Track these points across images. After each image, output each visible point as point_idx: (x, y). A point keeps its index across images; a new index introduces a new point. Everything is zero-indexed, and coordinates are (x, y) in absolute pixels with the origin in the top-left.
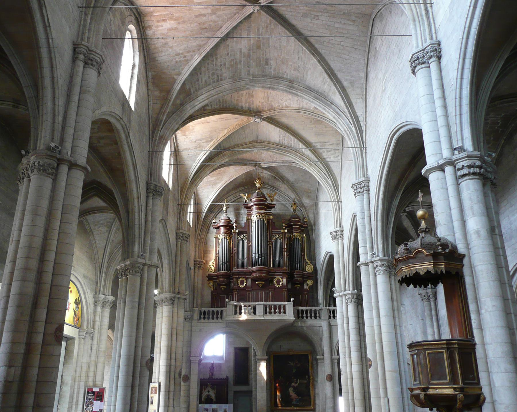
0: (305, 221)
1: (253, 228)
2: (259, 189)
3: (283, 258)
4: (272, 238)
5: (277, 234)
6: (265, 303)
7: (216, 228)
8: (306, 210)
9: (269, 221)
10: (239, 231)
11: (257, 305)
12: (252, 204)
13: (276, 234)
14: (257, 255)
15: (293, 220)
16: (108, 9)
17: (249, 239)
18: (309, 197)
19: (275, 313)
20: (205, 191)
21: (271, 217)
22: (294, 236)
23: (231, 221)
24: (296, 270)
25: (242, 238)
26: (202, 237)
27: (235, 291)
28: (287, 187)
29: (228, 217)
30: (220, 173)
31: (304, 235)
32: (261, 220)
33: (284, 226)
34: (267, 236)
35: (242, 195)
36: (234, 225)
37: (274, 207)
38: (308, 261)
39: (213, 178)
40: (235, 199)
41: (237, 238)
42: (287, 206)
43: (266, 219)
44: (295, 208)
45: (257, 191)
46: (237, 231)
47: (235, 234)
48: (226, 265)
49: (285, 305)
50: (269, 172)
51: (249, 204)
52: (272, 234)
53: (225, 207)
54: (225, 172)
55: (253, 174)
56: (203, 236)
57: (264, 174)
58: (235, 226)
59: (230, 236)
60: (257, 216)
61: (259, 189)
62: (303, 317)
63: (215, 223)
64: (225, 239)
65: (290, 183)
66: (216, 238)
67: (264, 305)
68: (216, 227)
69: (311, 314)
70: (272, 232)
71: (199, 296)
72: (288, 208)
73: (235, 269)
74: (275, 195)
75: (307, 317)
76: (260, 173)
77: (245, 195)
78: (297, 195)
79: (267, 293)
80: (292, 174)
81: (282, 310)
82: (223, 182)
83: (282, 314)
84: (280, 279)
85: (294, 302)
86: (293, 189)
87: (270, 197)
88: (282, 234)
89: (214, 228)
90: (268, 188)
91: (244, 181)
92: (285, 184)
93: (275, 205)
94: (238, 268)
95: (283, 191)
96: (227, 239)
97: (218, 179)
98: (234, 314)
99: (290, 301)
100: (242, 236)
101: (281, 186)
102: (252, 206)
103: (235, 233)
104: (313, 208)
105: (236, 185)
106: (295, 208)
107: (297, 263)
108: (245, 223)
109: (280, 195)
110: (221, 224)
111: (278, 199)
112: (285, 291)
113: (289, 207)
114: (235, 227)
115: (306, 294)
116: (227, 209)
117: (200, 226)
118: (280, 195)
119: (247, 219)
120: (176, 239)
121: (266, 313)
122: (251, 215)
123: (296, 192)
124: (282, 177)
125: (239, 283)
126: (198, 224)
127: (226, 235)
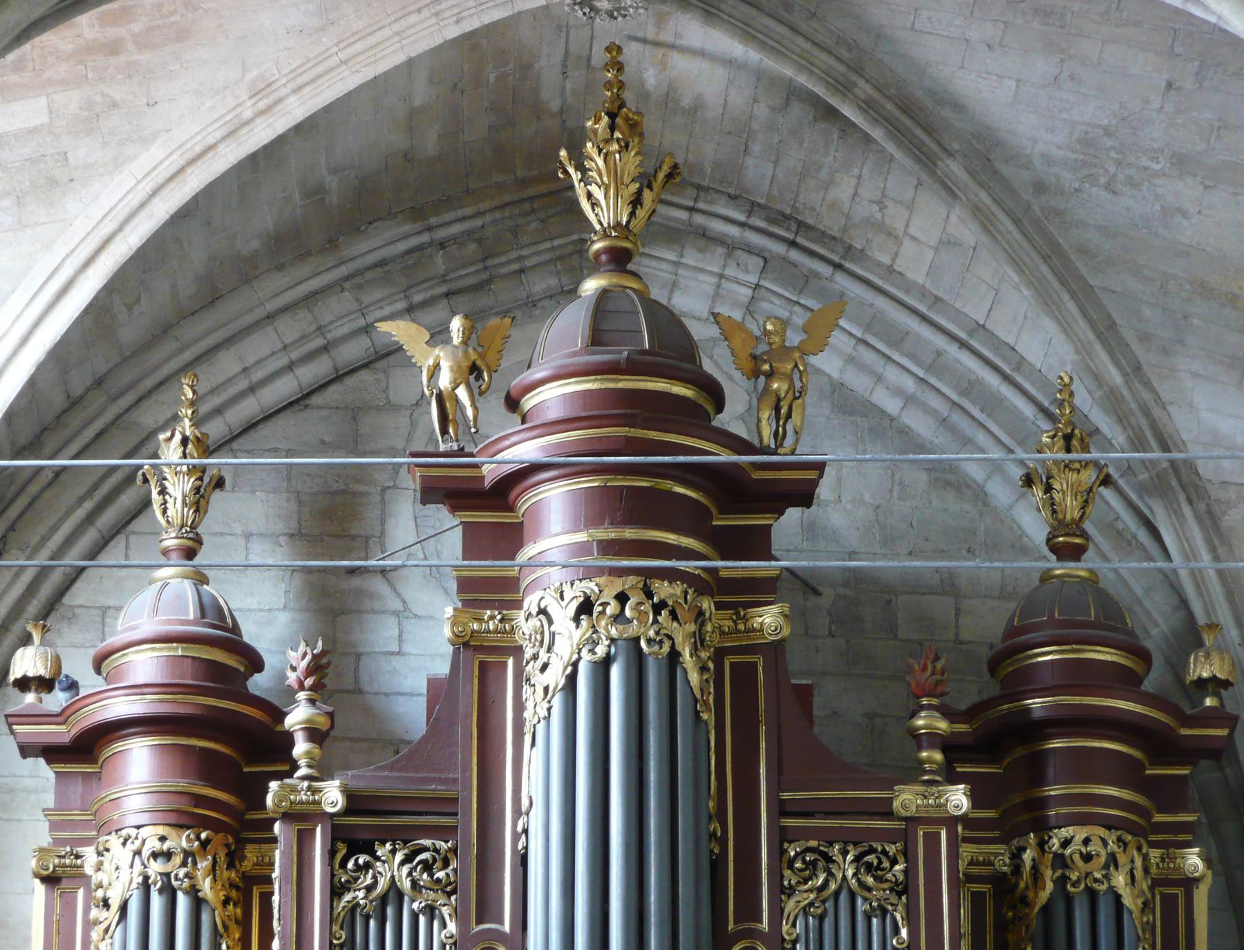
0: (1202, 669)
1: (533, 759)
2: (619, 259)
4: (781, 891)
5: (848, 839)
7: (52, 753)
8: (1211, 523)
9: (744, 675)
10: (356, 803)
12: (528, 450)
15: (1047, 655)
16: (533, 633)
17: (486, 907)
21: (769, 618)
22: (1061, 861)
23: (255, 662)
28: (967, 232)
29: (212, 611)
30: (113, 48)
31: (1193, 860)
32: (637, 662)
33: (935, 740)
34: (717, 866)
35: (400, 331)
36: (297, 716)
37: (804, 496)
40: (310, 373)
41: (336, 890)
42: (976, 472)
43: (699, 642)
44: (1071, 507)
45: (591, 286)
46: (332, 796)
47: (304, 840)
50: (747, 33)
51: (493, 448)
52: (781, 837)
53: (178, 488)
54: (182, 35)
55: (548, 64)
57: (679, 62)
58: (314, 734)
59: (234, 858)
60: (586, 607)
61: (619, 259)
63: (45, 684)
64: (169, 892)
66: (51, 880)
68: (62, 734)
70: (781, 809)
72: (979, 496)
74: (817, 338)
76: (632, 52)
77: (439, 335)
78: (1107, 332)
80: (1043, 67)
82: (156, 153)
86: (1054, 254)
87: (756, 368)
88: (905, 836)
89: (26, 750)
90: (731, 247)
91: (430, 143)
92: (949, 190)
95: (918, 276)
96: (198, 904)
97: (88, 123)
101: (895, 216)
102: (526, 473)
105: (315, 192)
106: (1071, 507)
108: (440, 693)
110: (122, 707)
111: (858, 382)
113: (1001, 493)
114: (301, 747)
116: (198, 502)
118: (875, 323)
119: (465, 644)
122: (511, 584)
123: (1084, 295)
124: (908, 106)
127: (181, 841)
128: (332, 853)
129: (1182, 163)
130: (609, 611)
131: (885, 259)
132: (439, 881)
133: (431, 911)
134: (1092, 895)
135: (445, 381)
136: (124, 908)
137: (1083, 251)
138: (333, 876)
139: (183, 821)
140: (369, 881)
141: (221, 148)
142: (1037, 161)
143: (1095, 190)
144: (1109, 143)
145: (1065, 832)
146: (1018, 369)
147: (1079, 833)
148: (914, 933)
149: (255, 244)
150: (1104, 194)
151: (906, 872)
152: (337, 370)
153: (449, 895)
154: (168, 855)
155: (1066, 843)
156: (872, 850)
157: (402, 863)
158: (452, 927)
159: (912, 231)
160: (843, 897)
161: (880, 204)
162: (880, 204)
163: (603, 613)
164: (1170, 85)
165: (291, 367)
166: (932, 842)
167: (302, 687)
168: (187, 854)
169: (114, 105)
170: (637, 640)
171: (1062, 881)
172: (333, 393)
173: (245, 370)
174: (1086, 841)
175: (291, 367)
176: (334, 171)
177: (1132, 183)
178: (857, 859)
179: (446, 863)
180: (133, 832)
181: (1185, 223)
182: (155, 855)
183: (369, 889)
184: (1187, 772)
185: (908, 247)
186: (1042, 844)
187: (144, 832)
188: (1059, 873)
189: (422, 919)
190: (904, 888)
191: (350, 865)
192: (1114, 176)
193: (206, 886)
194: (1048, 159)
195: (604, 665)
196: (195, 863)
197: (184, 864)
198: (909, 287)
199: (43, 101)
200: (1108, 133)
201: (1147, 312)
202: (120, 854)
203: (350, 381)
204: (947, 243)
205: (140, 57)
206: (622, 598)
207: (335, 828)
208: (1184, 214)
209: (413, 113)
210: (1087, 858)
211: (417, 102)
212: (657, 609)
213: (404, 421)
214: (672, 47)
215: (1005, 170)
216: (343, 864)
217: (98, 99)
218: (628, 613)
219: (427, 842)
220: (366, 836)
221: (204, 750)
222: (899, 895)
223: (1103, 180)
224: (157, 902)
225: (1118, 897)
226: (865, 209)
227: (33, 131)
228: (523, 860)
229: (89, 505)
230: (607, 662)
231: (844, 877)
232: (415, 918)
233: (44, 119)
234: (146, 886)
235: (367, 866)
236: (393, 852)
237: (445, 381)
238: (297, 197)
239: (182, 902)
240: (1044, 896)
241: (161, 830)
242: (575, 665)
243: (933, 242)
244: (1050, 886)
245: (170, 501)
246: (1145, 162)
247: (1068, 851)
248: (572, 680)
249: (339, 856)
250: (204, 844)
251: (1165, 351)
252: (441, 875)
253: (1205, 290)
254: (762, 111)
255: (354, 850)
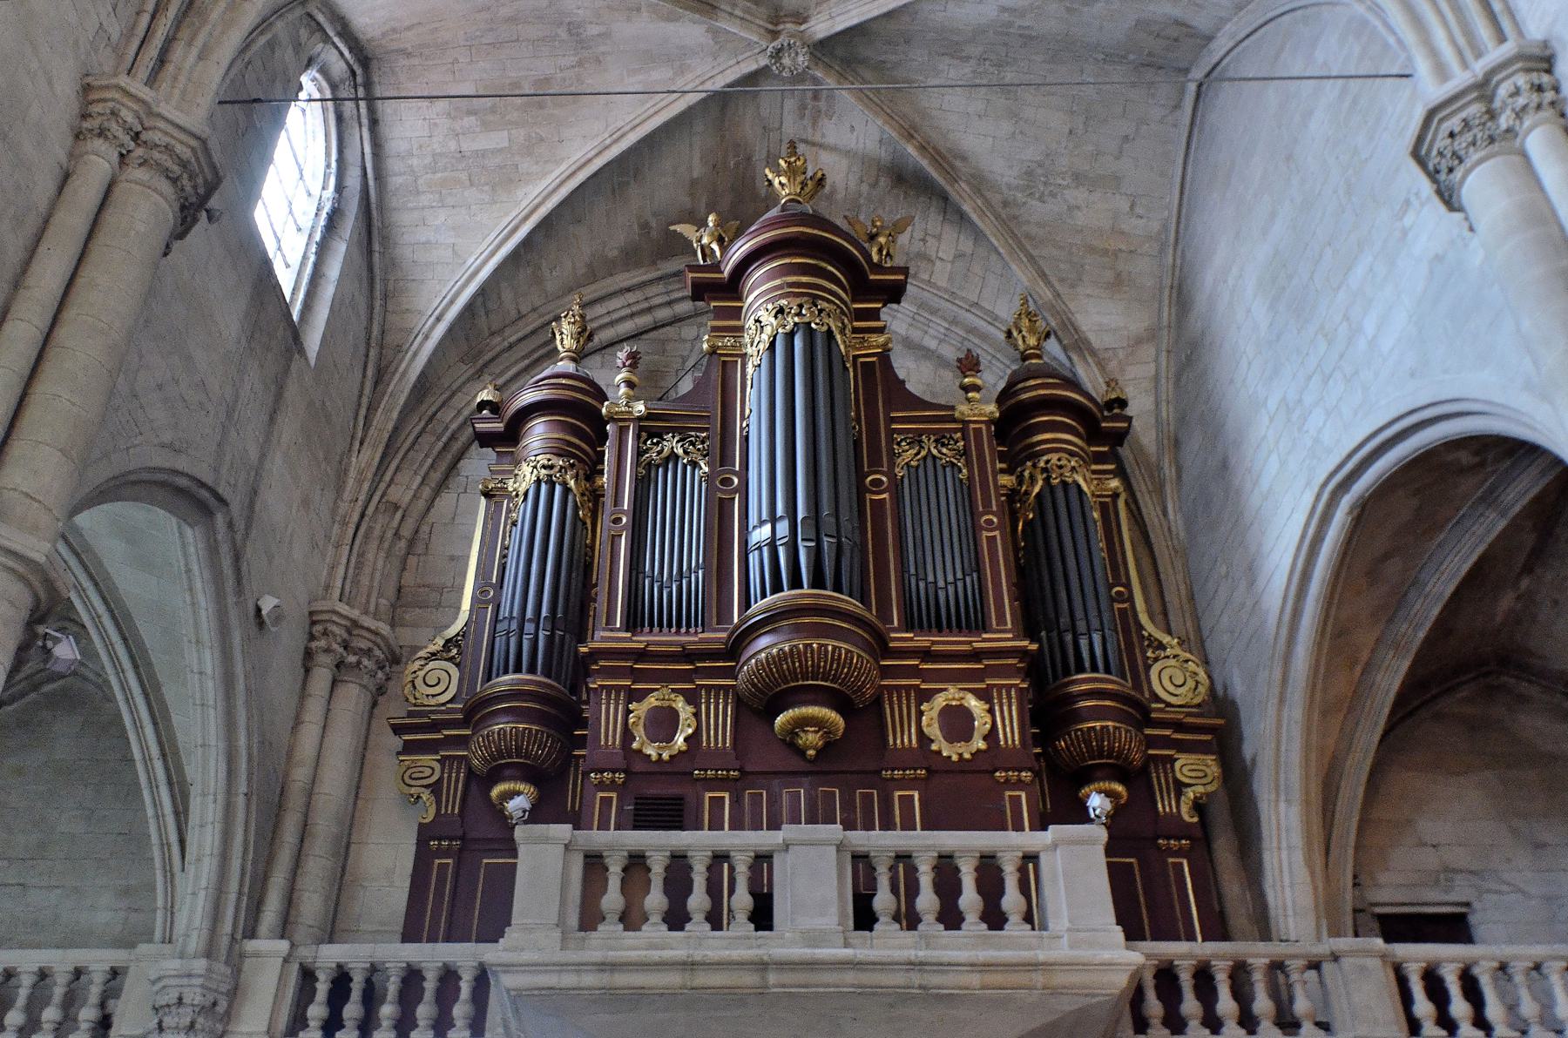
3: (979, 569)
6: (861, 839)
11: (786, 847)
13: (920, 433)
14: (783, 528)
17: (725, 458)
18: (1118, 283)
19: (951, 918)
20: (441, 217)
23: (603, 397)
24: (1081, 669)
25: (674, 457)
26: (395, 494)
27: (601, 786)
32: (810, 333)
34: (857, 444)
38: (1166, 639)
39: (498, 139)
40: (644, 321)
41: (639, 453)
47: (623, 431)
48: (550, 640)
49: (1031, 858)
56: (401, 493)
60: (781, 311)
62: (1175, 1022)
64: (551, 485)
65: (996, 199)
66: (487, 494)
67: (840, 847)
69: (1242, 994)
71: (317, 867)
73: (609, 634)
75: (1213, 1022)
76: (801, 148)
77: (702, 224)
79: (867, 799)
80: (1006, 127)
81: (1012, 900)
82: (563, 167)
83: (1015, 927)
84: (973, 703)
85: (1113, 822)
93: (905, 271)
94: (634, 621)
96: (567, 490)
97: (528, 149)
98: (573, 920)
99: (1080, 815)
100: (672, 444)
103: (621, 421)
104: (1148, 351)
107: (1081, 626)
109: (922, 305)
111: (915, 335)
112: (1020, 784)
115: (1179, 853)
117: (385, 421)
120: (78, 136)
121: (864, 918)
125: (640, 733)
126: (372, 408)
128: (638, 437)
129: (1078, 178)
130: (793, 311)
131: (926, 277)
132: (699, 450)
133: (695, 465)
134: (1064, 484)
135: (705, 241)
136: (526, 494)
137: (1028, 236)
138: (638, 447)
139: (562, 452)
140: (659, 449)
141: (595, 161)
142: (1004, 188)
143: (1034, 202)
144: (1040, 171)
145: (1045, 458)
146: (995, 320)
147: (1054, 457)
148: (970, 470)
149: (615, 253)
150: (1039, 204)
151: (964, 446)
152: (655, 322)
153: (705, 456)
154: (551, 467)
155: (1047, 462)
156: (945, 437)
157: (678, 442)
158: (706, 469)
159: (940, 254)
160: (929, 462)
161: (923, 240)
162: (923, 240)
163: (790, 312)
164: (1071, 132)
165: (632, 315)
166: (978, 432)
167: (624, 366)
168: (561, 467)
169: (542, 140)
170: (809, 323)
171: (1047, 480)
172: (652, 335)
173: (608, 313)
174: (1059, 460)
175: (632, 315)
176: (654, 214)
177: (1053, 195)
178: (936, 441)
179: (703, 442)
180: (533, 458)
181: (1080, 214)
182: (544, 467)
183: (659, 453)
184: (1106, 449)
185: (938, 263)
186: (1034, 466)
187: (538, 458)
188: (1045, 475)
189: (689, 467)
190: (965, 452)
191: (649, 442)
192: (1043, 193)
193: (572, 483)
194: (1009, 186)
195: (790, 336)
196: (566, 472)
197: (560, 471)
198: (939, 289)
199: (506, 132)
200: (1040, 165)
201: (1062, 266)
202: (526, 469)
203: (661, 331)
204: (960, 256)
205: (556, 112)
206: (801, 306)
207: (641, 429)
208: (1078, 208)
209: (694, 183)
210: (1061, 467)
211: (695, 175)
212: (820, 311)
213: (688, 345)
214: (821, 146)
215: (988, 195)
216: (645, 443)
217: (534, 135)
218: (804, 312)
219: (693, 433)
220: (659, 431)
221: (572, 424)
222: (961, 456)
223: (1037, 196)
224: (544, 487)
225: (1079, 486)
226: (917, 246)
227: (500, 150)
228: (746, 439)
229: (527, 362)
230: (790, 336)
231: (929, 449)
232: (685, 467)
233: (506, 144)
234: (538, 481)
235: (657, 444)
236: (673, 437)
237: (705, 241)
238: (636, 227)
239: (558, 488)
240: (1037, 489)
241: (548, 456)
242: (775, 337)
243: (951, 258)
244: (1040, 483)
245: (565, 337)
246: (1061, 182)
247: (1049, 466)
248: (772, 345)
249: (642, 440)
250: (572, 466)
251: (1072, 286)
252: (700, 446)
253: (1091, 249)
254: (865, 188)
255: (651, 436)
